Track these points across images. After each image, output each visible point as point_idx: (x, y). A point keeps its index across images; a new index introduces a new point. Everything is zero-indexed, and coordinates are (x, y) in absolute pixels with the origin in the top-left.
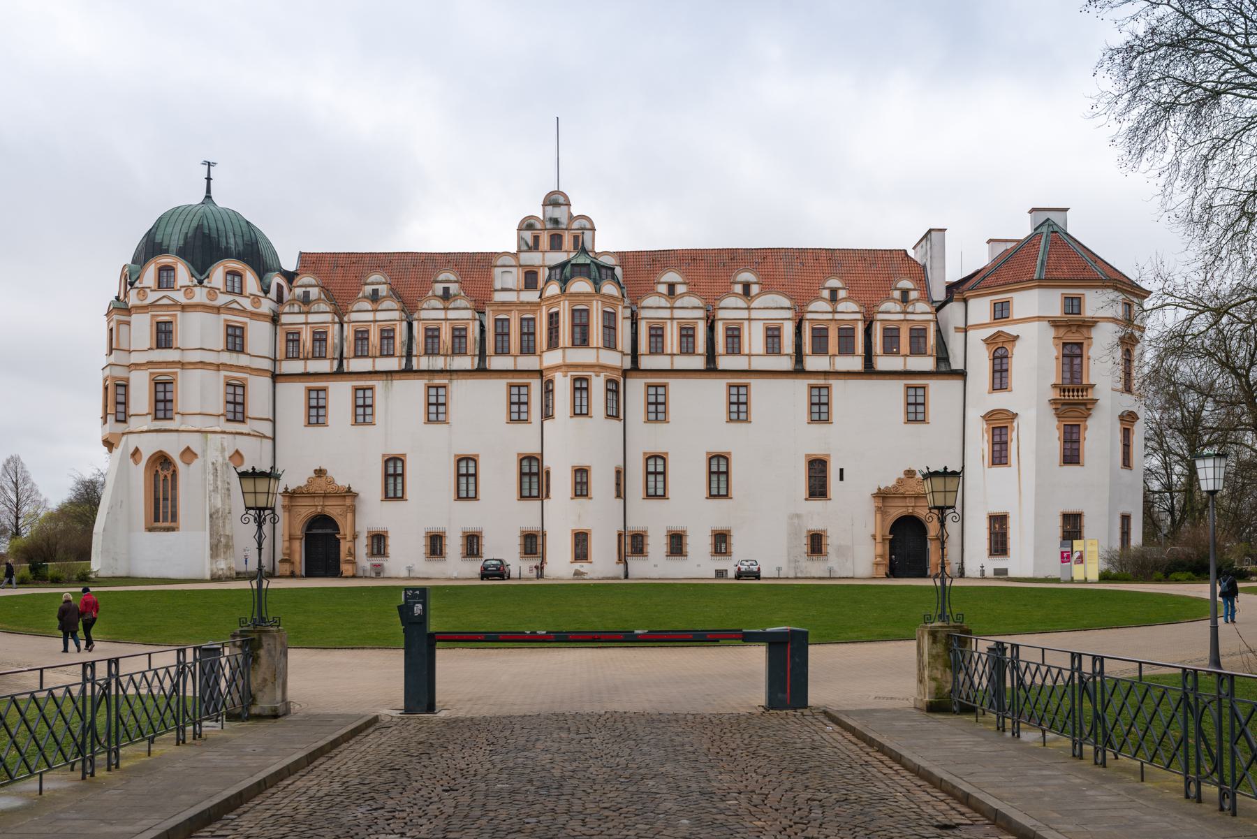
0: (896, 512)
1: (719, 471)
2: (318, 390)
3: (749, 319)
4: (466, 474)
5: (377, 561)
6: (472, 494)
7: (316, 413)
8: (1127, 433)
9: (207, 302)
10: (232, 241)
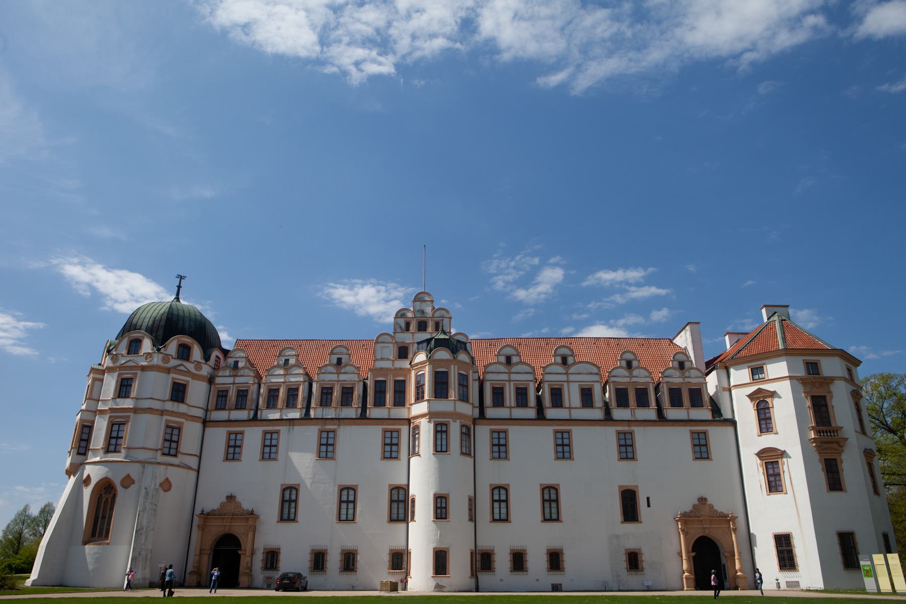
0: (696, 534)
1: (550, 501)
2: (236, 434)
3: (568, 381)
4: (347, 500)
5: (270, 573)
7: (233, 451)
9: (161, 364)
10: (187, 324)
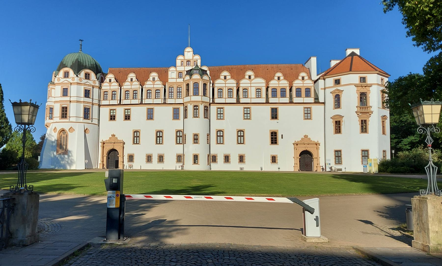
4: (159, 137)
5: (130, 163)
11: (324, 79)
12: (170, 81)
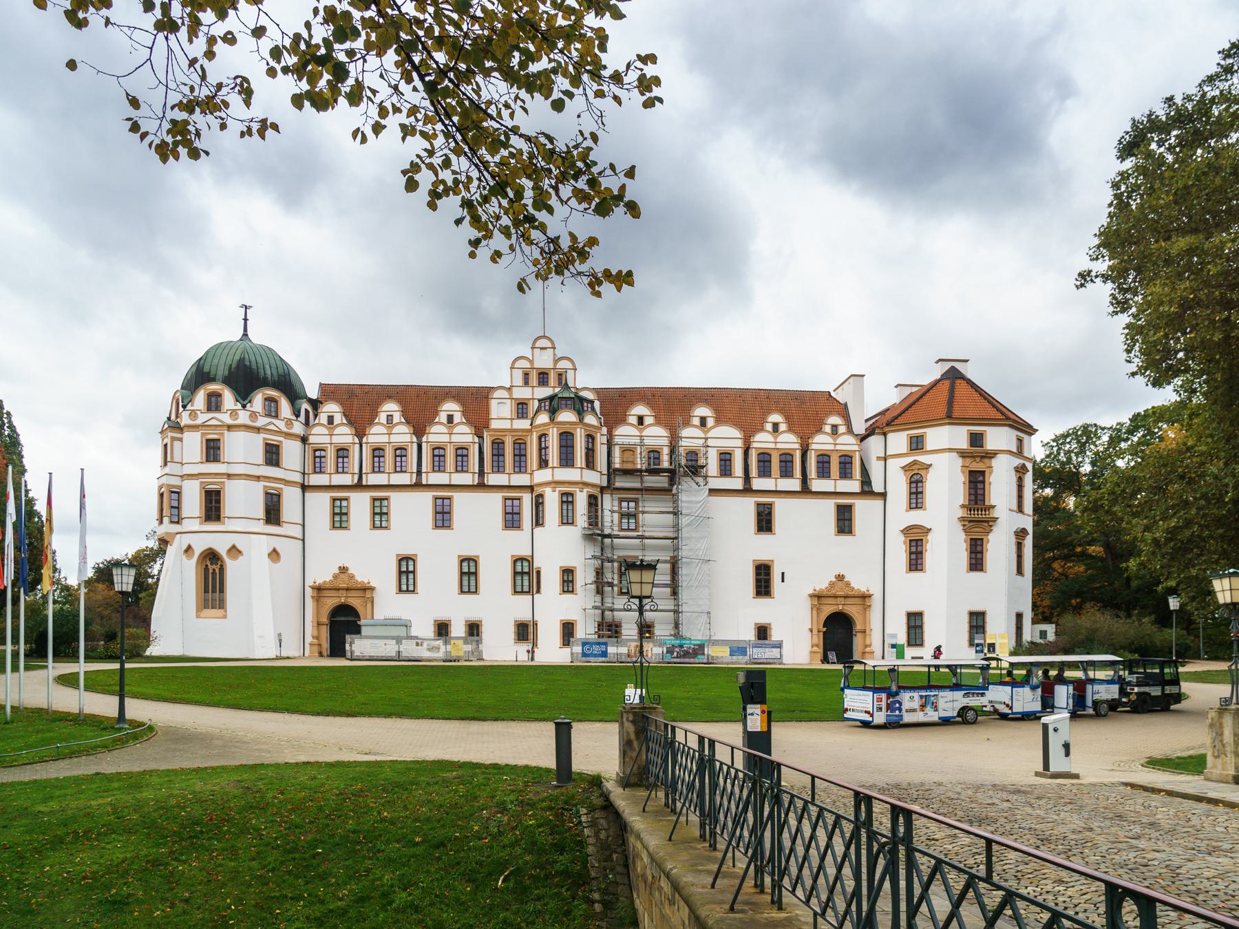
0: (828, 610)
4: (469, 573)
6: (473, 589)
7: (339, 518)
8: (1019, 546)
10: (268, 372)
11: (885, 434)
12: (494, 425)
